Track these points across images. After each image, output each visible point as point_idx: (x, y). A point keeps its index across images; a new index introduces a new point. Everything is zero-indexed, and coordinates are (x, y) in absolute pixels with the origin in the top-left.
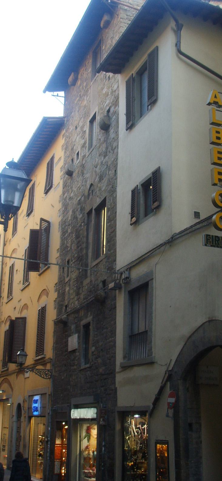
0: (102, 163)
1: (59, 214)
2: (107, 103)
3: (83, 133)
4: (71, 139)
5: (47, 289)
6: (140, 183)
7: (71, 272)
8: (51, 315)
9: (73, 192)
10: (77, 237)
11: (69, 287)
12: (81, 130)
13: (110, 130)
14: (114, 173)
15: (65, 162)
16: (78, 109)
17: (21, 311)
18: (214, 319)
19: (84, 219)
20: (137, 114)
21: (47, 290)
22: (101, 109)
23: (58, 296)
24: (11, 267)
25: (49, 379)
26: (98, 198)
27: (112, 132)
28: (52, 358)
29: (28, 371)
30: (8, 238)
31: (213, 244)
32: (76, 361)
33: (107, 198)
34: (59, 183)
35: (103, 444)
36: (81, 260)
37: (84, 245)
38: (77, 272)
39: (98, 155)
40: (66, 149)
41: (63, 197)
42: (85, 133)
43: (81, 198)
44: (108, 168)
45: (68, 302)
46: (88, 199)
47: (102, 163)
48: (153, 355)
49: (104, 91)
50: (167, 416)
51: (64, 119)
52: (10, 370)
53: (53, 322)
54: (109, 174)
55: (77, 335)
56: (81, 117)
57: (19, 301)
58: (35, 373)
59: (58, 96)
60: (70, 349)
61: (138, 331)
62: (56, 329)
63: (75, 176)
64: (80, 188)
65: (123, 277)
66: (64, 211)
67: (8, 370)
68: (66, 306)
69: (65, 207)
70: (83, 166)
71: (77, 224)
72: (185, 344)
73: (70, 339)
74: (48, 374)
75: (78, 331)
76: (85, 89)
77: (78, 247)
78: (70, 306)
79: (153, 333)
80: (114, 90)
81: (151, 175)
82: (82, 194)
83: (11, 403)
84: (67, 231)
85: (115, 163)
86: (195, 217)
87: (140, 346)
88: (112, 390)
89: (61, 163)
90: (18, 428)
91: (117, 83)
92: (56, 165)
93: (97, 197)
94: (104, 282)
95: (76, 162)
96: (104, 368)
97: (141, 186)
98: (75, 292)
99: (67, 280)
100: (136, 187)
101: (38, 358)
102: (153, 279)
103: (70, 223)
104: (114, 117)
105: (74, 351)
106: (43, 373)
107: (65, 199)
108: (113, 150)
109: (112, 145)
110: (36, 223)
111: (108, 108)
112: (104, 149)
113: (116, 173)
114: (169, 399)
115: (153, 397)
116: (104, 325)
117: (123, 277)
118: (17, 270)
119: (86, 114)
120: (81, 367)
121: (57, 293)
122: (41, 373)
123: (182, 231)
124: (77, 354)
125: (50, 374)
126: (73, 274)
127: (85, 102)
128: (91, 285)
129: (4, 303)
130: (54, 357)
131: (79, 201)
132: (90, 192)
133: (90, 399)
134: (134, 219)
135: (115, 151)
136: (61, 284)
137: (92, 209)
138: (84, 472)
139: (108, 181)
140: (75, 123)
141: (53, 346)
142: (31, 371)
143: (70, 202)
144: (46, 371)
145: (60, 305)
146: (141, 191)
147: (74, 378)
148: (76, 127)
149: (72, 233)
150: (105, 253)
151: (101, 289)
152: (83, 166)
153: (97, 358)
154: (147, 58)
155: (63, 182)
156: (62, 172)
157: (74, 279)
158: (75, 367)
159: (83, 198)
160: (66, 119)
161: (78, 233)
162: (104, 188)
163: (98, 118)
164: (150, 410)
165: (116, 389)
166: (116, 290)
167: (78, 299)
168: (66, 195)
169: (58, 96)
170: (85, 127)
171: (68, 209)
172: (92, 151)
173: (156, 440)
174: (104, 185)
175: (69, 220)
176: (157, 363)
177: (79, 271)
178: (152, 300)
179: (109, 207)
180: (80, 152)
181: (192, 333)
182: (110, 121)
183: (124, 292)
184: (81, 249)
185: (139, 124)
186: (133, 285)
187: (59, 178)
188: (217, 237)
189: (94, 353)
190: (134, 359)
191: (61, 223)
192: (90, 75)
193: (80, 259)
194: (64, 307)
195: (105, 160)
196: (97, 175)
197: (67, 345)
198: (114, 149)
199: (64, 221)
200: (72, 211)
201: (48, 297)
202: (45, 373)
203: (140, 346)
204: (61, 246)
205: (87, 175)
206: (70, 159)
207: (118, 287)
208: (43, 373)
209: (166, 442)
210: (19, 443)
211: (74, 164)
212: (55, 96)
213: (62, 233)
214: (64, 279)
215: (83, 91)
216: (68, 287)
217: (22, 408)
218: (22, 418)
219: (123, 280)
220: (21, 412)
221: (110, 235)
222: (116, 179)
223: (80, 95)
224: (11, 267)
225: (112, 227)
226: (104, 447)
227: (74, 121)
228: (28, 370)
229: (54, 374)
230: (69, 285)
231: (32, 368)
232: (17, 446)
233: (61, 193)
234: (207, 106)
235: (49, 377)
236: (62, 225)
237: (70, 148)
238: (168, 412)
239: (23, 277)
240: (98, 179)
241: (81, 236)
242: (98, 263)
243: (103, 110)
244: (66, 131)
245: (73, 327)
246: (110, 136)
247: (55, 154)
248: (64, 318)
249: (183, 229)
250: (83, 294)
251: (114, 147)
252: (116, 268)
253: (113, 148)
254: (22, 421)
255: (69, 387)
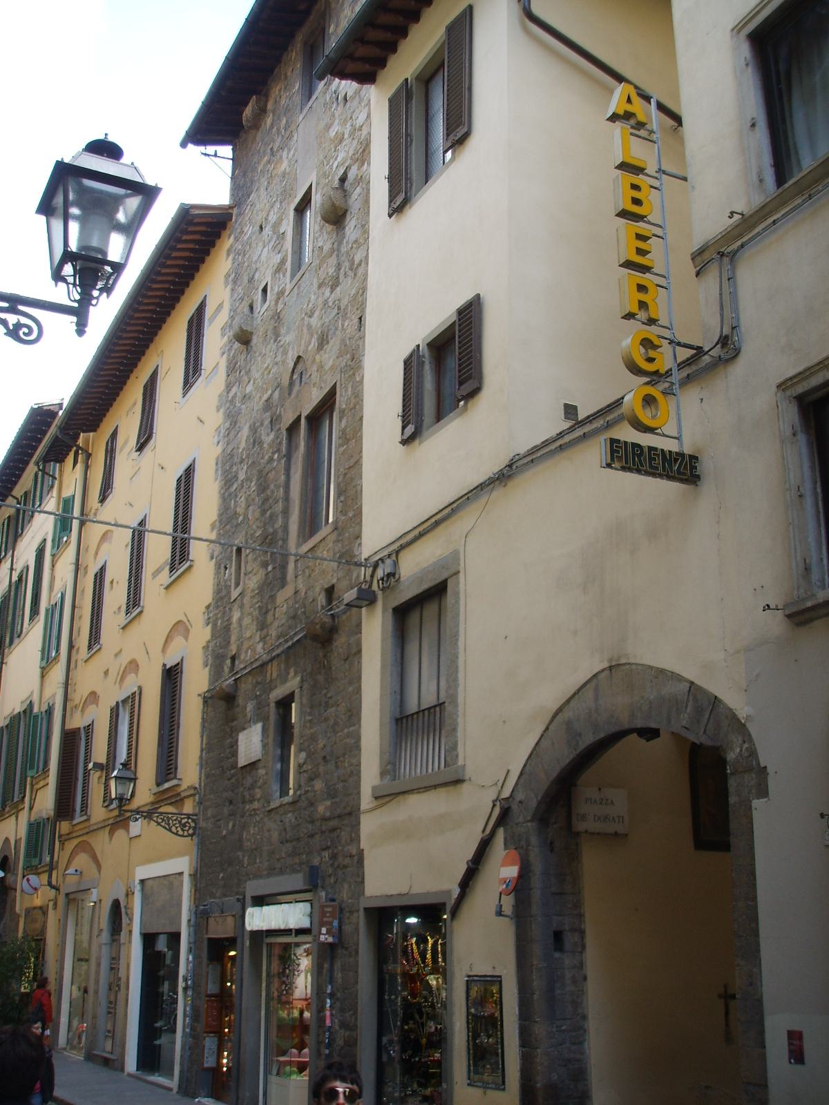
0: (325, 304)
1: (216, 437)
2: (339, 159)
3: (278, 239)
4: (247, 256)
5: (185, 620)
6: (423, 340)
7: (245, 574)
8: (196, 682)
9: (252, 382)
10: (263, 488)
11: (241, 611)
12: (274, 233)
13: (346, 223)
14: (357, 324)
15: (232, 314)
16: (266, 183)
17: (122, 676)
18: (623, 661)
19: (280, 443)
20: (416, 174)
21: (185, 623)
22: (325, 175)
23: (212, 636)
24: (99, 574)
25: (190, 838)
26: (315, 389)
27: (352, 228)
28: (197, 786)
29: (138, 816)
30: (91, 508)
31: (626, 463)
32: (257, 790)
33: (337, 383)
34: (218, 364)
35: (329, 991)
36: (271, 541)
37: (279, 507)
38: (262, 572)
39: (315, 285)
40: (235, 282)
41: (228, 397)
42: (283, 238)
43: (271, 395)
44: (341, 313)
45: (239, 649)
46: (290, 394)
47: (325, 304)
48: (460, 762)
49: (332, 133)
50: (499, 913)
51: (230, 211)
52: (93, 821)
53: (200, 698)
54: (343, 329)
55: (259, 726)
56: (275, 202)
57: (116, 655)
58: (157, 822)
59: (215, 155)
60: (242, 761)
61: (419, 707)
62: (207, 715)
63: (256, 344)
64: (268, 370)
65: (380, 573)
66: (228, 429)
67: (88, 820)
68: (233, 659)
69: (232, 418)
70: (279, 317)
71: (262, 458)
72: (547, 729)
73: (242, 737)
74: (187, 824)
75: (264, 719)
76: (283, 133)
77: (264, 512)
78: (242, 657)
79: (460, 708)
80: (357, 126)
81: (454, 318)
82: (276, 384)
83: (95, 900)
84: (235, 476)
85: (360, 299)
86: (565, 418)
87: (431, 736)
88: (351, 856)
89: (224, 317)
90: (113, 959)
91: (367, 108)
92: (210, 323)
93: (312, 386)
94: (330, 592)
95: (261, 309)
96: (328, 803)
97: (426, 347)
98: (255, 623)
99: (235, 594)
100: (414, 350)
101: (161, 788)
102: (459, 572)
103: (244, 457)
104: (358, 190)
105: (253, 766)
106: (174, 822)
107: (232, 401)
108: (354, 268)
109: (351, 257)
110: (160, 465)
111: (342, 171)
112: (331, 271)
113: (362, 322)
114: (503, 869)
115: (462, 869)
116: (331, 698)
117: (380, 573)
118: (112, 582)
119: (286, 194)
120: (271, 804)
121: (209, 628)
122: (171, 821)
123: (535, 447)
124: (262, 772)
125: (193, 825)
126: (249, 579)
127: (284, 166)
128: (296, 602)
129: (80, 663)
130: (203, 784)
131: (267, 401)
132: (295, 377)
133: (297, 881)
134: (410, 429)
135: (360, 273)
136: (222, 601)
137: (299, 418)
138: (277, 1060)
139: (340, 344)
140: (259, 218)
141: (201, 757)
142: (145, 819)
143: (243, 406)
144: (183, 816)
145: (219, 656)
146: (427, 360)
147: (252, 832)
148: (261, 227)
149: (248, 479)
150: (331, 520)
151: (323, 607)
152: (279, 317)
153: (311, 779)
154: (444, 38)
155: (228, 361)
156: (226, 337)
157: (253, 591)
158: (256, 805)
159: (277, 394)
160: (235, 212)
161: (263, 478)
162: (331, 363)
163: (317, 199)
164: (453, 901)
165: (361, 853)
166: (362, 607)
167: (263, 639)
168: (234, 389)
169: (215, 155)
170: (284, 222)
171: (238, 425)
172: (299, 280)
173: (469, 976)
174: (329, 357)
175: (240, 450)
176: (470, 779)
177: (267, 569)
178: (457, 625)
179: (344, 406)
180: (271, 284)
181: (564, 700)
182: (346, 201)
183: (383, 613)
184: (271, 516)
185: (418, 202)
186: (407, 592)
187: (218, 352)
188: (639, 446)
189: (305, 767)
190: (402, 777)
191: (220, 459)
192: (297, 99)
193: (267, 541)
194: (229, 662)
195: (333, 295)
196: (312, 335)
197: (235, 754)
198: (357, 267)
199: (229, 454)
200: (250, 427)
201: (187, 640)
202: (180, 822)
203: (431, 736)
204: (220, 515)
205: (288, 338)
206: (246, 304)
207: (367, 598)
208: (174, 822)
209: (495, 979)
210: (116, 996)
211: (256, 314)
212: (208, 155)
213: (223, 482)
214: (229, 593)
215: (279, 140)
216: (239, 609)
217: (123, 910)
218: (123, 933)
219: (380, 582)
220: (121, 919)
221: (345, 474)
222: (362, 338)
223: (272, 149)
224: (99, 574)
225: (352, 456)
226: (330, 999)
227: (254, 212)
228: (138, 814)
229: (202, 824)
230: (242, 606)
231: (149, 814)
232: (111, 1003)
233: (223, 389)
234: (608, 122)
235: (191, 831)
236: (224, 464)
237: (246, 279)
238: (501, 903)
239: (126, 596)
240: (317, 344)
241: (272, 487)
242: (314, 547)
243: (330, 178)
244: (236, 239)
245: (250, 707)
246: (347, 238)
247: (207, 298)
248: (227, 686)
249: (538, 441)
250: (276, 624)
251: (356, 263)
252: (361, 553)
253: (353, 264)
254: (122, 941)
255: (240, 853)
